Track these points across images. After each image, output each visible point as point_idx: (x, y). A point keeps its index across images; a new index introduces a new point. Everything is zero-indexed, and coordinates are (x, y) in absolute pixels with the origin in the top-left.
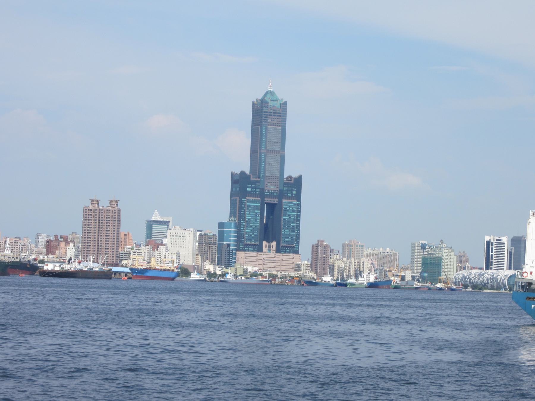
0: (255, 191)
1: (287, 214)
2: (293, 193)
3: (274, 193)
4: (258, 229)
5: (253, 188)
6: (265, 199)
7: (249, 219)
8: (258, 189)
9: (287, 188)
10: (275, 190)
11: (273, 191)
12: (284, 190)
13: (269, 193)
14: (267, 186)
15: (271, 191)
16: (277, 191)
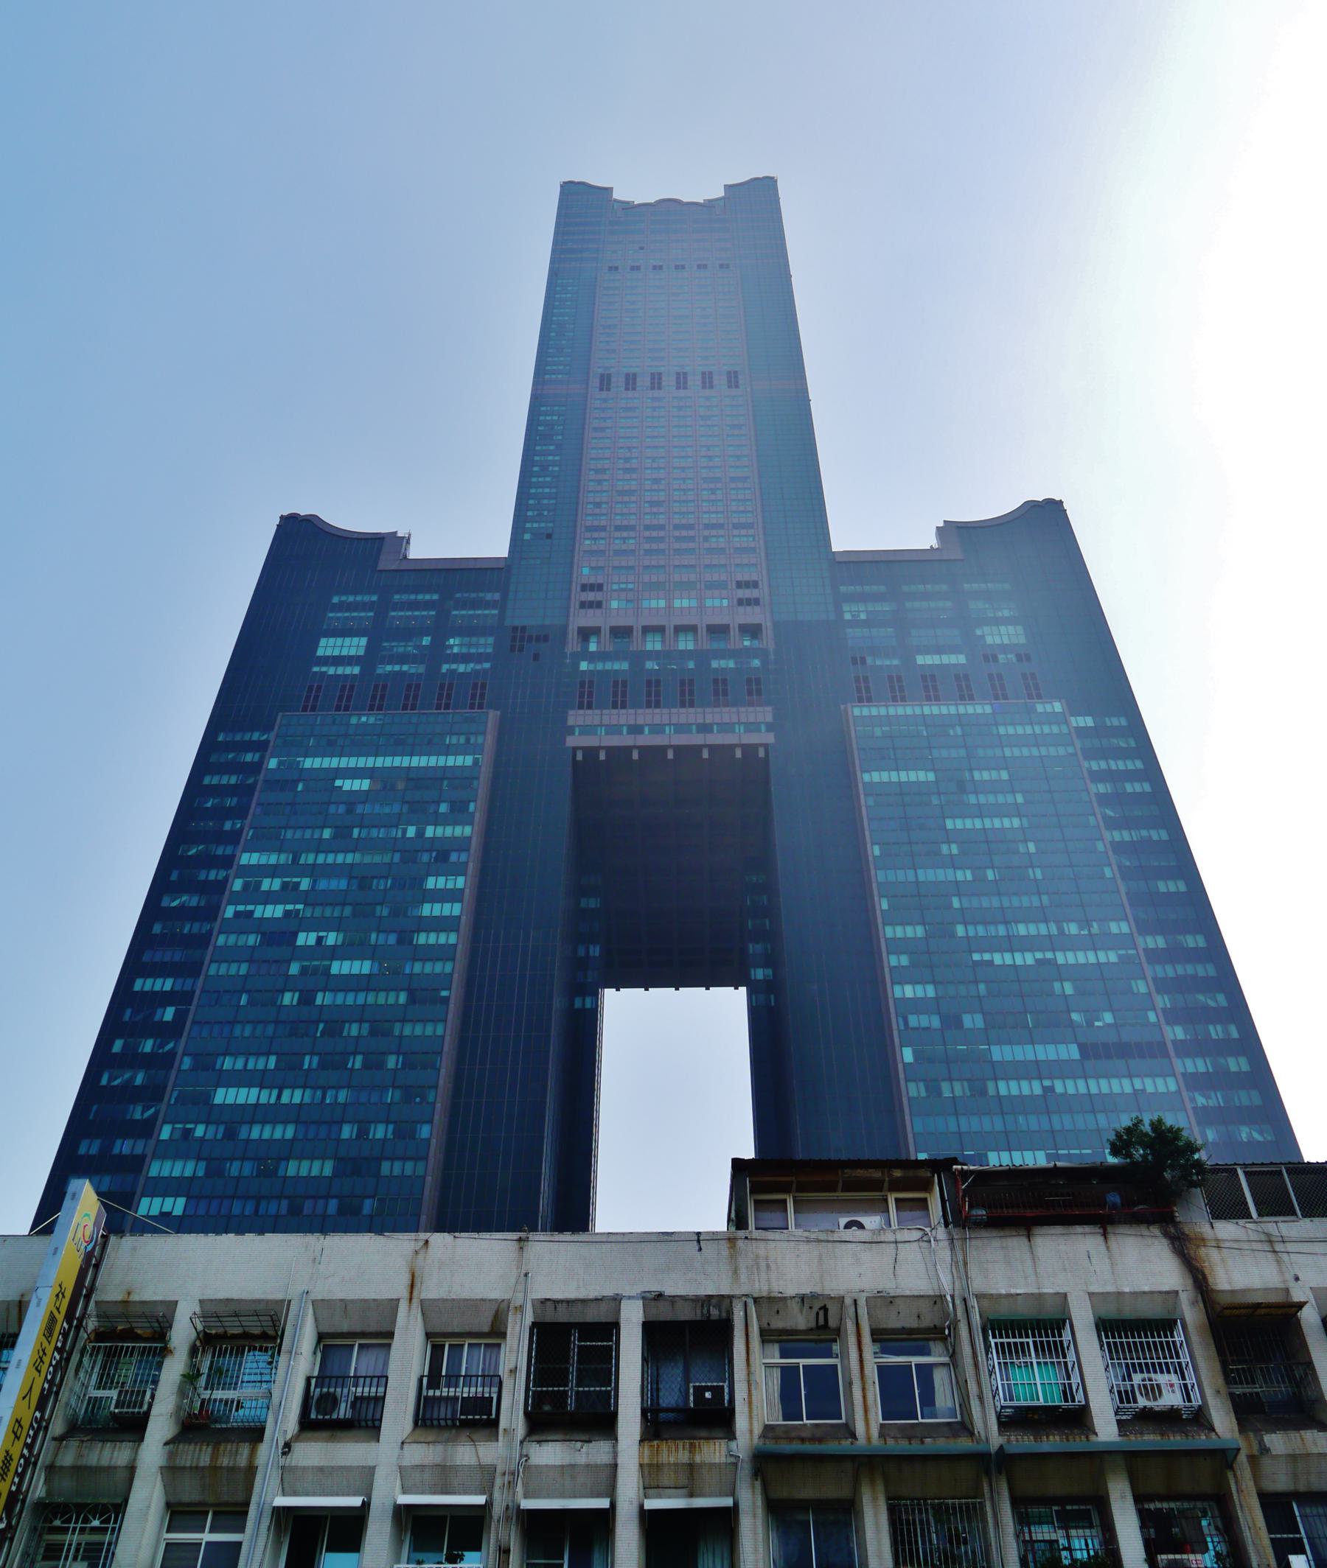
0: (437, 654)
1: (949, 837)
2: (989, 640)
3: (702, 657)
4: (418, 1057)
5: (408, 633)
6: (576, 717)
7: (279, 936)
8: (468, 631)
9: (886, 607)
10: (718, 631)
11: (686, 644)
12: (855, 623)
13: (638, 658)
14: (591, 596)
15: (653, 644)
16: (753, 631)
